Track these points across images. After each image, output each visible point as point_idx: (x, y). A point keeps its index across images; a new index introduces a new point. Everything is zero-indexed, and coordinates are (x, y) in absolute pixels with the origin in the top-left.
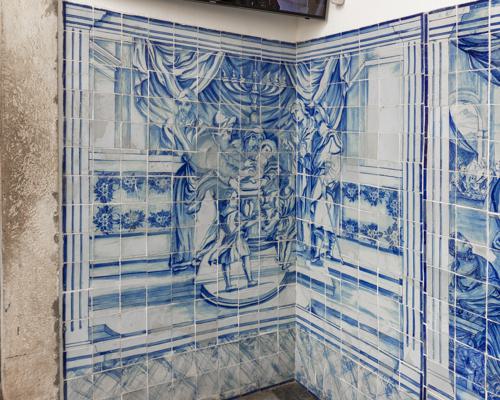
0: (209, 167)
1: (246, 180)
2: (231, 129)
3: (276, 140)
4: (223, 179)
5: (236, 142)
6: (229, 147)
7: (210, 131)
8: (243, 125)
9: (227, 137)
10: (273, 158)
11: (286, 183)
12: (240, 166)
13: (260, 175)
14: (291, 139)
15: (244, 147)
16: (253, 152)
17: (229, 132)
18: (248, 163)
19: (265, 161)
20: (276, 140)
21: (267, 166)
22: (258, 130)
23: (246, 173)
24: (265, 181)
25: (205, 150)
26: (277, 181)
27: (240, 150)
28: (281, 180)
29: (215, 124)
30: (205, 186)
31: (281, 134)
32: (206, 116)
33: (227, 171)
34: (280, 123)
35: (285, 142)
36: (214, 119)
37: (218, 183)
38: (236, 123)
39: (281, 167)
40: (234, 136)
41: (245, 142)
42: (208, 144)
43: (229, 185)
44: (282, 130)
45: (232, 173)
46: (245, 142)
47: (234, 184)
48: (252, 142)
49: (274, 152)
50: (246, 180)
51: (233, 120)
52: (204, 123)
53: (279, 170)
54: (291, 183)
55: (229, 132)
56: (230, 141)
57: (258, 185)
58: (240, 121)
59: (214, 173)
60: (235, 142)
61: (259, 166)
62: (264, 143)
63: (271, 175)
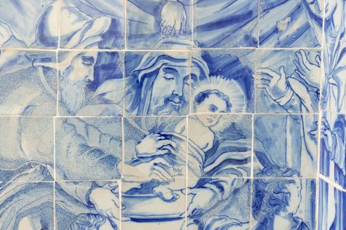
0: (28, 153)
1: (144, 190)
2: (93, 52)
3: (246, 80)
4: (70, 188)
5: (115, 89)
6: (88, 102)
7: (31, 58)
8: (134, 37)
9: (84, 73)
10: (235, 131)
11: (279, 203)
12: (124, 152)
13: (189, 178)
14: (300, 74)
15: (138, 102)
16: (166, 116)
17: (87, 60)
18: (149, 145)
19: (207, 140)
20: (246, 80)
21: (211, 153)
22: (186, 50)
23: (144, 172)
24: (204, 198)
25: (16, 111)
26: (246, 197)
27: (123, 108)
28: (259, 194)
29: (44, 38)
30: (16, 206)
31: (261, 60)
32: (19, 18)
33: (88, 166)
34: (259, 27)
35: (278, 82)
36: (42, 26)
37: (55, 198)
38: (113, 32)
39: (261, 157)
40: (104, 70)
41: (140, 84)
42: (26, 94)
43: (90, 205)
44: (268, 47)
45: (100, 173)
46: (140, 84)
47: (104, 201)
48: (162, 86)
49: (239, 113)
50: (144, 190)
51: (102, 24)
52: (13, 37)
53: (254, 165)
54: (297, 204)
55: (87, 60)
56: (93, 85)
57: (182, 206)
58: (124, 28)
59: (44, 170)
60: (107, 87)
61: (184, 152)
62: (203, 87)
63: (227, 179)
